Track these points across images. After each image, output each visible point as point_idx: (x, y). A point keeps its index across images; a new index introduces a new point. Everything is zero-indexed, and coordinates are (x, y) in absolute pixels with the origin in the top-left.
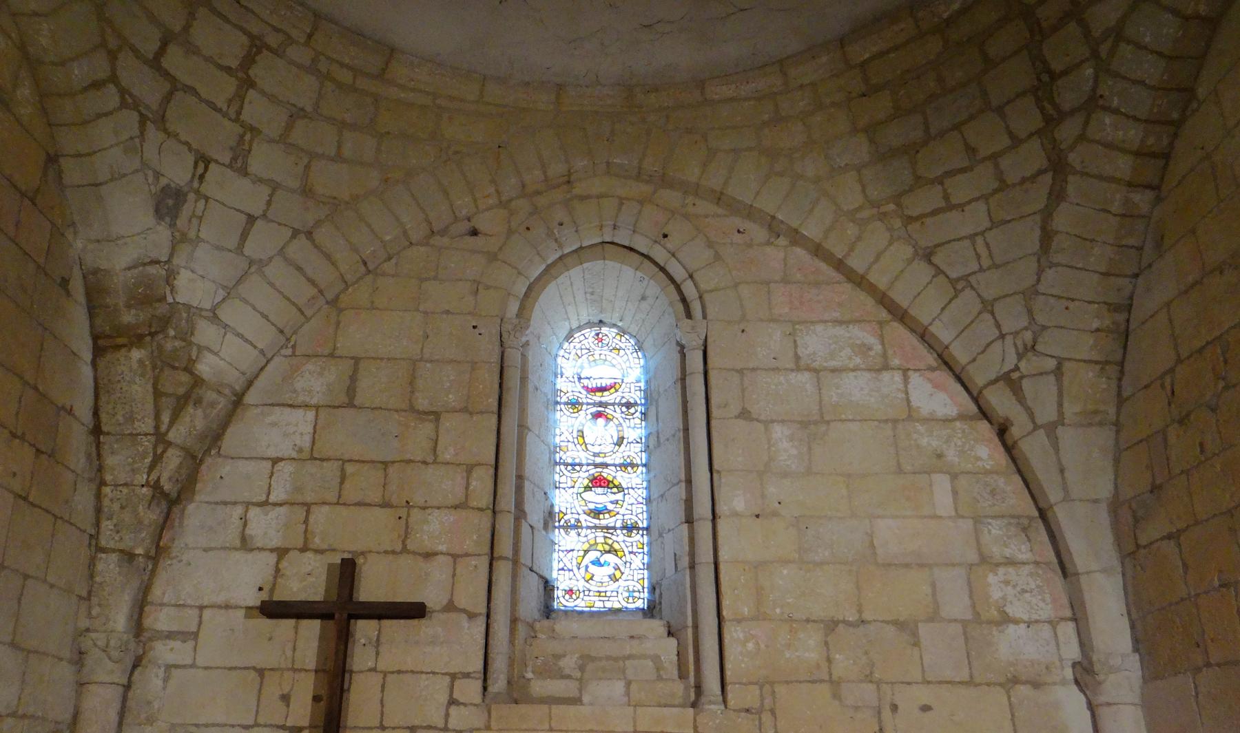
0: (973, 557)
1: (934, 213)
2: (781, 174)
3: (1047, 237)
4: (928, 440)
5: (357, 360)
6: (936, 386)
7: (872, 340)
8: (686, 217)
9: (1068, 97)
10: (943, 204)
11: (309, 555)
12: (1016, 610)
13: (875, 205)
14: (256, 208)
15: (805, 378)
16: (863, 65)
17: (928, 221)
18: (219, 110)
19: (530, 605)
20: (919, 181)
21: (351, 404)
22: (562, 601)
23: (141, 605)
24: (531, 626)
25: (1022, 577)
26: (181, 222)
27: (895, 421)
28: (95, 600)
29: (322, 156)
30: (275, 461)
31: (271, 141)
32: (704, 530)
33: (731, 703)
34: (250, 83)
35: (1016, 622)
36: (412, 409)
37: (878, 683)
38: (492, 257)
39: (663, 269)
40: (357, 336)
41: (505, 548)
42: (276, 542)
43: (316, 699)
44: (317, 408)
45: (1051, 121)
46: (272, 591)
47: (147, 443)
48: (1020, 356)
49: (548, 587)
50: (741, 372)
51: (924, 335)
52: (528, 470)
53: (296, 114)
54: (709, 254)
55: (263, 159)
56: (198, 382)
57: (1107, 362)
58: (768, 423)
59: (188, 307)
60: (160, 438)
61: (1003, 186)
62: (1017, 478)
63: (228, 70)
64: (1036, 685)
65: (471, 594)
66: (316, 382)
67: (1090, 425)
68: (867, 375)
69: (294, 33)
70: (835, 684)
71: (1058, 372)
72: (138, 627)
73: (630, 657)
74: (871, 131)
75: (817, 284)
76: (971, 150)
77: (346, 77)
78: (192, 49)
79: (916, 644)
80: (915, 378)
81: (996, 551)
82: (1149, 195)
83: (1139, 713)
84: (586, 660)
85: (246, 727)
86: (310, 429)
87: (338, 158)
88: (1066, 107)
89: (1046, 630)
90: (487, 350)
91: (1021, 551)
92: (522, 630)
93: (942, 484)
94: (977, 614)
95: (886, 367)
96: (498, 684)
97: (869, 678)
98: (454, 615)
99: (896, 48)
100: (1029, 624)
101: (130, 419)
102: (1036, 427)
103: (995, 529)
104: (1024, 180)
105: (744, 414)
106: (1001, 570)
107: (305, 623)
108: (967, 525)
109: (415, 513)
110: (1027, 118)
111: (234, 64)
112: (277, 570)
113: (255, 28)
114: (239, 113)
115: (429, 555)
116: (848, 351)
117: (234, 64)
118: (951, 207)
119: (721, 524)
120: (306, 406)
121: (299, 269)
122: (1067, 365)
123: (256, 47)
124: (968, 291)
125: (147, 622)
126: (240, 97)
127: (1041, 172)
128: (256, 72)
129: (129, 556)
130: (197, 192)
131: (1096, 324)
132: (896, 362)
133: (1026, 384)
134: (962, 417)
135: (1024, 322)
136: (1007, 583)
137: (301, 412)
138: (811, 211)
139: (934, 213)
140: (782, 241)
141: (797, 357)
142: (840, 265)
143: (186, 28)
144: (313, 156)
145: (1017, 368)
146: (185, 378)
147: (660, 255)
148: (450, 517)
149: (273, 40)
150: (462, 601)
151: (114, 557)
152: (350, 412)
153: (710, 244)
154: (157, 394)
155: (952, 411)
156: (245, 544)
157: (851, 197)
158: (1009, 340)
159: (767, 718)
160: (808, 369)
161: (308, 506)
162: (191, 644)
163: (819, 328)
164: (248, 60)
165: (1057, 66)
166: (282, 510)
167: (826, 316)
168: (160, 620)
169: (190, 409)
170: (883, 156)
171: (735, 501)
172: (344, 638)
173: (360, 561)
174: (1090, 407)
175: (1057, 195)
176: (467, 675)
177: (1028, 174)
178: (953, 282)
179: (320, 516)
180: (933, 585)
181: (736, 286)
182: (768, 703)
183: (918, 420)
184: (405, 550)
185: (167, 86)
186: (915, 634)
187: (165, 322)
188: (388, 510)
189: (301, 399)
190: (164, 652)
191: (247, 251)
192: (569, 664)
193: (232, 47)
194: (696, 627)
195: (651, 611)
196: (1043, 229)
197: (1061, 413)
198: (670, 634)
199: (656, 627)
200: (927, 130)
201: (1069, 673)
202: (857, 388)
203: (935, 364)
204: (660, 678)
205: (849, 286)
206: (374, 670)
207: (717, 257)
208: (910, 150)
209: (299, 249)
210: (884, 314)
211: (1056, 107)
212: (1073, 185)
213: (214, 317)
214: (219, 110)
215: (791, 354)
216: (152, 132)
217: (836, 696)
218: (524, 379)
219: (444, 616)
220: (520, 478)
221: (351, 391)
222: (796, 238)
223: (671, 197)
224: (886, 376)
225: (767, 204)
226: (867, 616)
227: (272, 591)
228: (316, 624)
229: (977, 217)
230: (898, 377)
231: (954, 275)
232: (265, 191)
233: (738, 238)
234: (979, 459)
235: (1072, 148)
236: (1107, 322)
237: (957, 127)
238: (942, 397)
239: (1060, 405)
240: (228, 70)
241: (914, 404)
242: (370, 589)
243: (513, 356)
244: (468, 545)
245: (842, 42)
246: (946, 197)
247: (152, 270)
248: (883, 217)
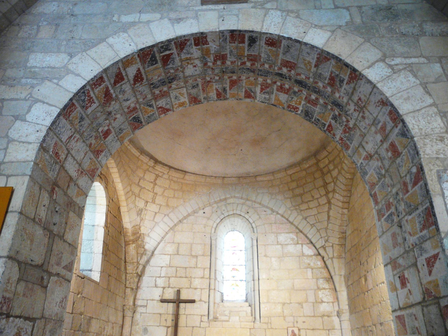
0: (316, 288)
1: (307, 209)
2: (274, 199)
3: (329, 217)
4: (307, 261)
5: (179, 244)
6: (309, 248)
7: (295, 237)
8: (253, 208)
9: (331, 187)
10: (308, 207)
11: (170, 288)
12: (325, 300)
13: (294, 206)
14: (157, 211)
15: (279, 246)
16: (290, 175)
17: (306, 211)
18: (149, 191)
19: (218, 300)
20: (303, 202)
21: (178, 254)
22: (225, 298)
23: (135, 299)
24: (218, 304)
25: (327, 292)
26: (142, 216)
27: (300, 256)
28: (126, 298)
29: (170, 197)
30: (162, 267)
31: (160, 195)
32: (256, 282)
33: (261, 321)
34: (155, 184)
35: (325, 302)
36: (191, 255)
37: (294, 317)
38: (208, 219)
39: (247, 220)
40: (179, 238)
41: (212, 287)
42: (163, 286)
43: (172, 320)
44: (170, 255)
45: (327, 193)
46: (162, 296)
47: (135, 264)
48: (325, 242)
49: (222, 294)
50: (265, 245)
51: (306, 236)
52: (217, 269)
53: (166, 189)
54: (258, 217)
55: (159, 200)
56: (145, 250)
57: (342, 245)
58: (271, 258)
59: (143, 234)
60: (138, 263)
61: (319, 205)
62: (326, 269)
63: (152, 182)
64: (328, 316)
65: (205, 298)
66: (170, 249)
67: (340, 258)
68: (293, 246)
69: (165, 172)
70: (284, 317)
71: (332, 246)
72: (134, 304)
73: (241, 311)
74: (293, 190)
75: (282, 224)
76: (313, 197)
77: (175, 179)
78: (144, 180)
79: (302, 308)
80: (304, 246)
81: (321, 286)
82: (347, 210)
83: (349, 322)
84: (231, 312)
85: (158, 326)
86: (169, 260)
87: (174, 197)
88: (330, 190)
89: (331, 304)
90: (208, 241)
91: (326, 286)
92: (216, 305)
93: (309, 271)
94: (316, 301)
95: (298, 243)
96: (211, 317)
97: (292, 316)
98: (201, 302)
99: (297, 172)
100: (328, 303)
101: (132, 259)
102: (329, 258)
103: (321, 281)
104: (323, 204)
105: (266, 256)
106: (322, 291)
107: (169, 304)
108: (315, 280)
109: (193, 279)
110: (323, 192)
111: (153, 181)
112: (163, 292)
113: (157, 173)
114: (153, 191)
115: (196, 289)
116: (289, 240)
117: (153, 181)
118: (309, 208)
119: (260, 281)
120: (168, 254)
121: (166, 223)
122: (334, 245)
123: (157, 176)
124: (314, 227)
125: (136, 303)
126: (154, 187)
127: (326, 203)
128: (157, 182)
129: (132, 289)
130: (145, 209)
131: (339, 236)
132: (300, 242)
133: (327, 248)
134: (314, 255)
135: (325, 235)
136: (323, 293)
137: (166, 256)
138: (280, 207)
139: (307, 209)
140: (275, 213)
141: (278, 242)
142: (287, 220)
143: (144, 176)
144: (168, 197)
145: (325, 245)
146: (143, 249)
147: (247, 216)
148: (200, 280)
149: (160, 175)
150: (203, 299)
151: (129, 289)
152: (178, 256)
153: (258, 215)
154: (137, 253)
155: (312, 254)
156: (156, 286)
157: (289, 204)
158: (323, 239)
159: (269, 324)
160: (280, 244)
161: (169, 277)
162: (145, 308)
163: (283, 234)
164: (156, 179)
165: (327, 181)
166: (164, 278)
167: (284, 232)
168: (139, 303)
169: (144, 256)
170: (294, 196)
171: (263, 276)
172: (178, 307)
173: (181, 290)
174: (339, 254)
175: (330, 209)
176: (204, 315)
177: (324, 203)
178: (311, 225)
179: (172, 280)
180: (307, 295)
181: (264, 224)
182: (269, 321)
183: (305, 256)
184: (190, 287)
185: (140, 188)
186: (302, 306)
187: (139, 237)
188: (187, 279)
189: (167, 253)
190: (140, 310)
191: (155, 220)
192: (227, 313)
193: (153, 177)
194: (254, 304)
196: (328, 215)
197: (334, 256)
198: (250, 306)
199: (247, 304)
200: (304, 191)
201: (336, 313)
202: (291, 249)
203: (308, 242)
204: (247, 316)
205: (290, 224)
206: (184, 314)
207: (260, 218)
208: (301, 195)
209: (166, 219)
210: (298, 231)
211: (328, 190)
212: (333, 207)
213: (149, 236)
214: (149, 191)
215: (276, 241)
216: (137, 198)
217: (284, 320)
218: (216, 247)
219: (199, 302)
220: (215, 270)
221: (178, 251)
222: (278, 213)
223: (249, 203)
224: (298, 246)
225: (271, 206)
226: (292, 302)
227: (162, 296)
228: (172, 304)
229: (314, 211)
230: (300, 246)
231: (311, 223)
232: (158, 206)
233: (265, 213)
234: (318, 265)
235: (331, 199)
236: (341, 236)
237: (310, 191)
238: (310, 250)
239: (333, 254)
240: (152, 182)
241: (304, 252)
242: (183, 296)
243: (213, 242)
244: (204, 287)
245: (286, 169)
246: (309, 206)
247: (136, 227)
248: (296, 209)
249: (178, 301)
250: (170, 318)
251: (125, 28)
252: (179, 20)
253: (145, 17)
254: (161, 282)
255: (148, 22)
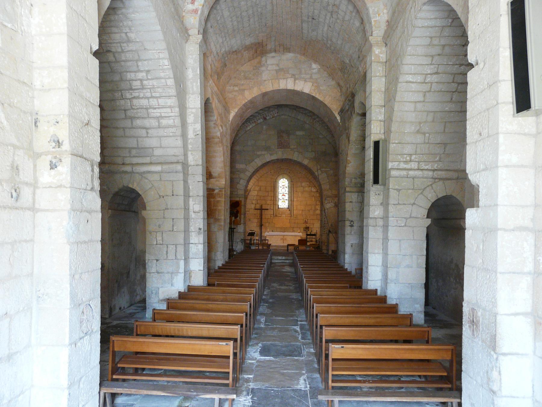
19: (277, 208)
65: (272, 208)
66: (257, 188)
171: (295, 200)
172: (262, 212)
190: (248, 213)
195: (288, 208)
202: (307, 189)
242: (263, 208)
249: (261, 209)
250: (259, 216)
251: (259, 156)
252: (271, 155)
253: (263, 153)
254: (254, 202)
255: (264, 155)
